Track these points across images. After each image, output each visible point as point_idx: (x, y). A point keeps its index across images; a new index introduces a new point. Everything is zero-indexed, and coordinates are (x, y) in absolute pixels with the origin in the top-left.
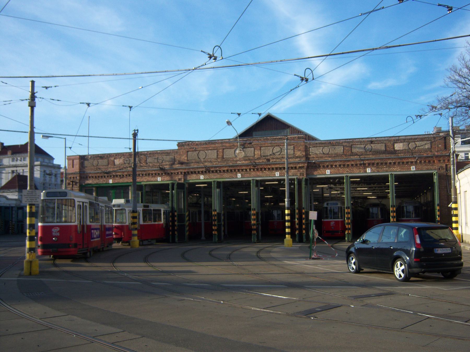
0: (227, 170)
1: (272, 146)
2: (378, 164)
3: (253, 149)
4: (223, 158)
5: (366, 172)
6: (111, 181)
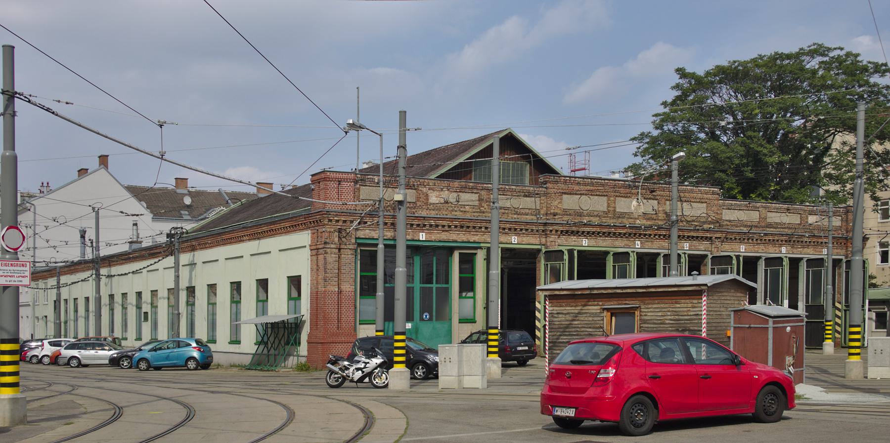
0: (625, 234)
5: (781, 252)
6: (422, 236)
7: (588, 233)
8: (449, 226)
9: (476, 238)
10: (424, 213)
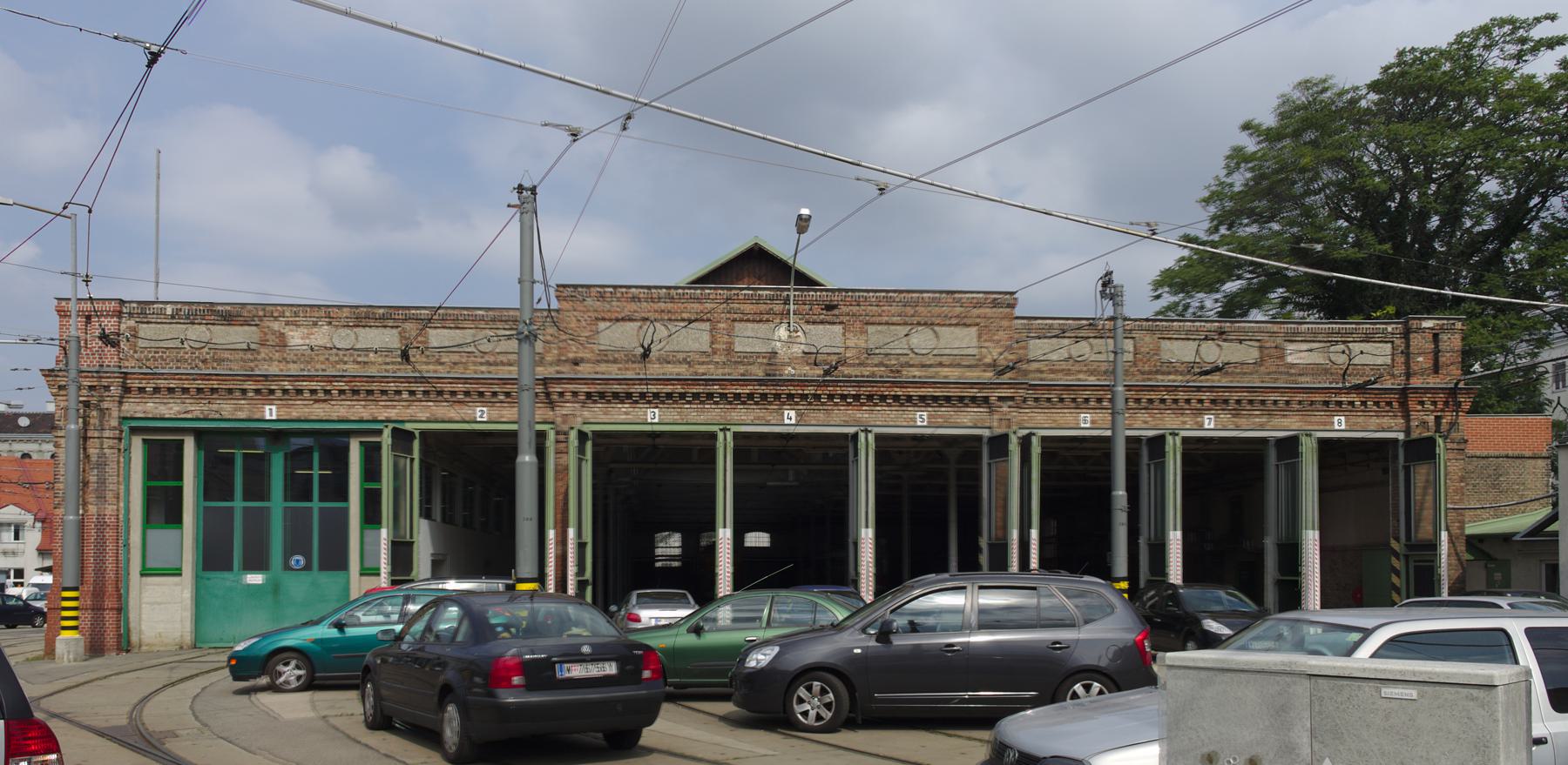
0: (750, 396)
1: (906, 324)
2: (1238, 402)
3: (838, 329)
4: (729, 351)
6: (271, 412)
7: (656, 395)
8: (327, 392)
9: (392, 414)
10: (274, 369)
